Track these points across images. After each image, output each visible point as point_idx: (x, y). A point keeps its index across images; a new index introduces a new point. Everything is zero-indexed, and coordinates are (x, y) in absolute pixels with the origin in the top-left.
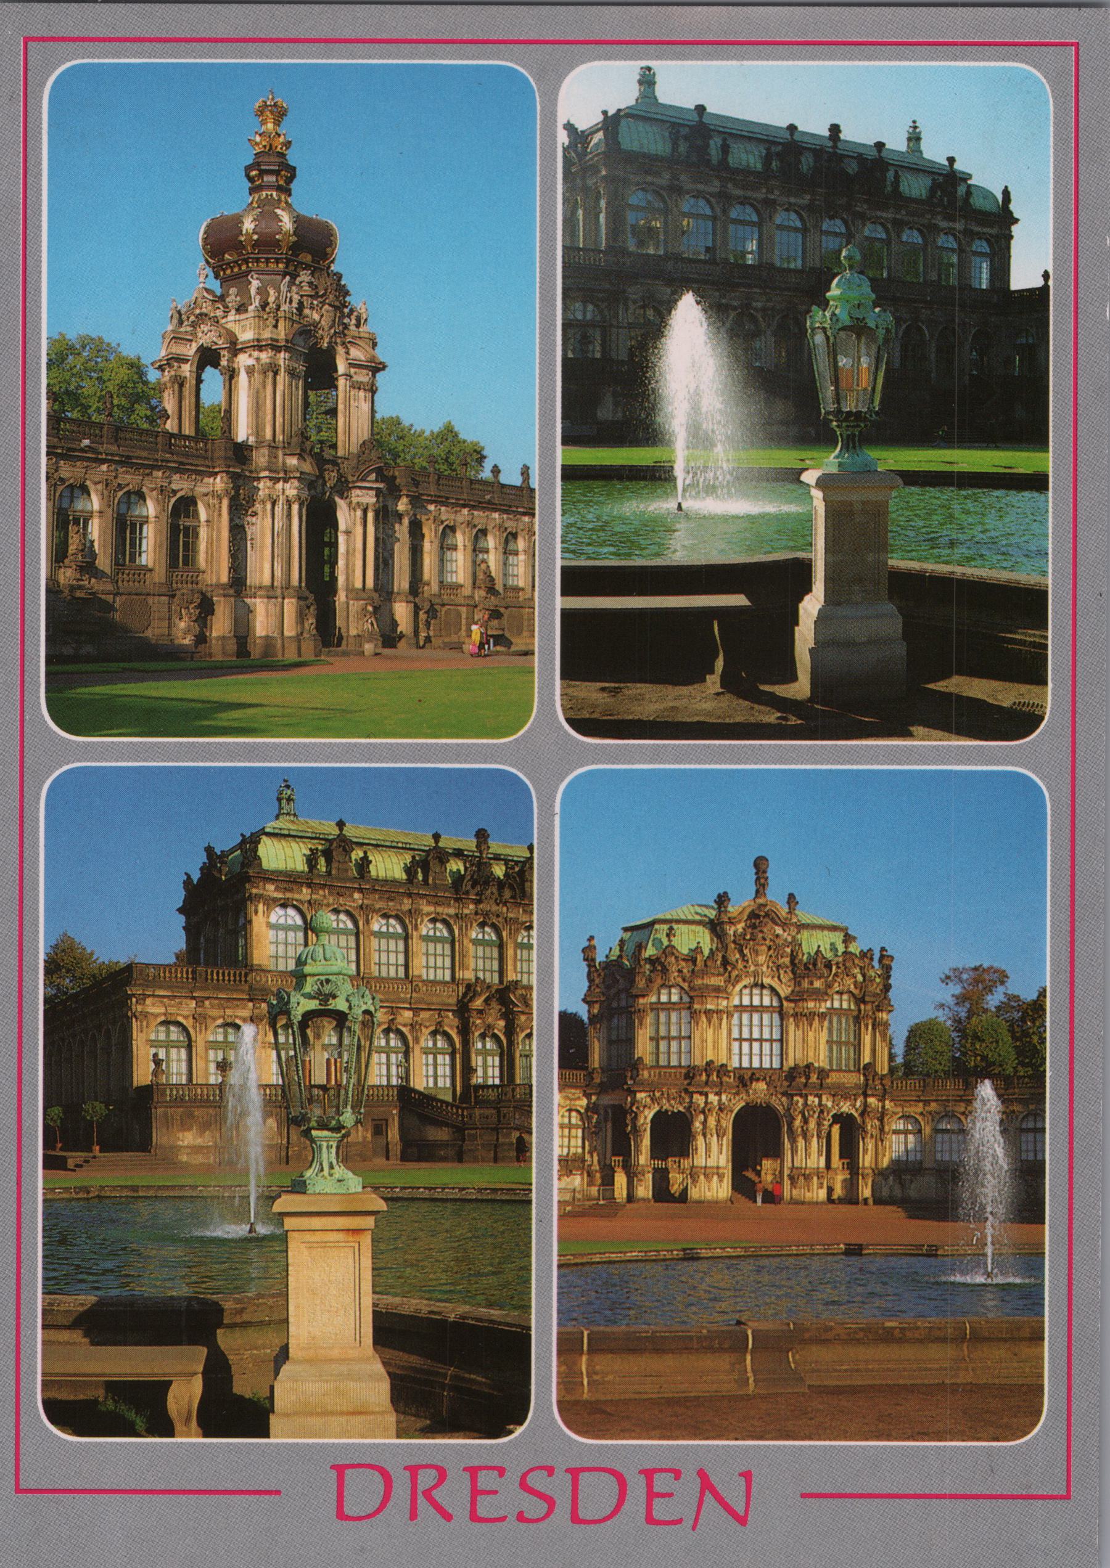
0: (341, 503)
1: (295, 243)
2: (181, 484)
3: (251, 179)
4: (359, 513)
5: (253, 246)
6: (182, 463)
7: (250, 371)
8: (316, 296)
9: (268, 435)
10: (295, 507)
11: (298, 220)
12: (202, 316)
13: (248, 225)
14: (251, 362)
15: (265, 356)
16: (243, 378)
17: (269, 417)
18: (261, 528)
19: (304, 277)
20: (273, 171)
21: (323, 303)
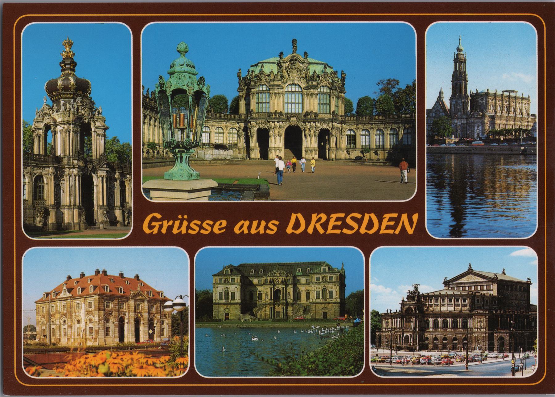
0: (94, 175)
1: (76, 88)
2: (37, 171)
3: (62, 67)
4: (100, 179)
5: (62, 90)
6: (37, 164)
7: (61, 132)
8: (82, 106)
9: (67, 153)
10: (77, 178)
11: (77, 80)
12: (45, 114)
13: (60, 83)
14: (61, 129)
15: (66, 126)
16: (59, 135)
17: (68, 147)
18: (65, 185)
19: (79, 99)
20: (69, 64)
21: (86, 107)
